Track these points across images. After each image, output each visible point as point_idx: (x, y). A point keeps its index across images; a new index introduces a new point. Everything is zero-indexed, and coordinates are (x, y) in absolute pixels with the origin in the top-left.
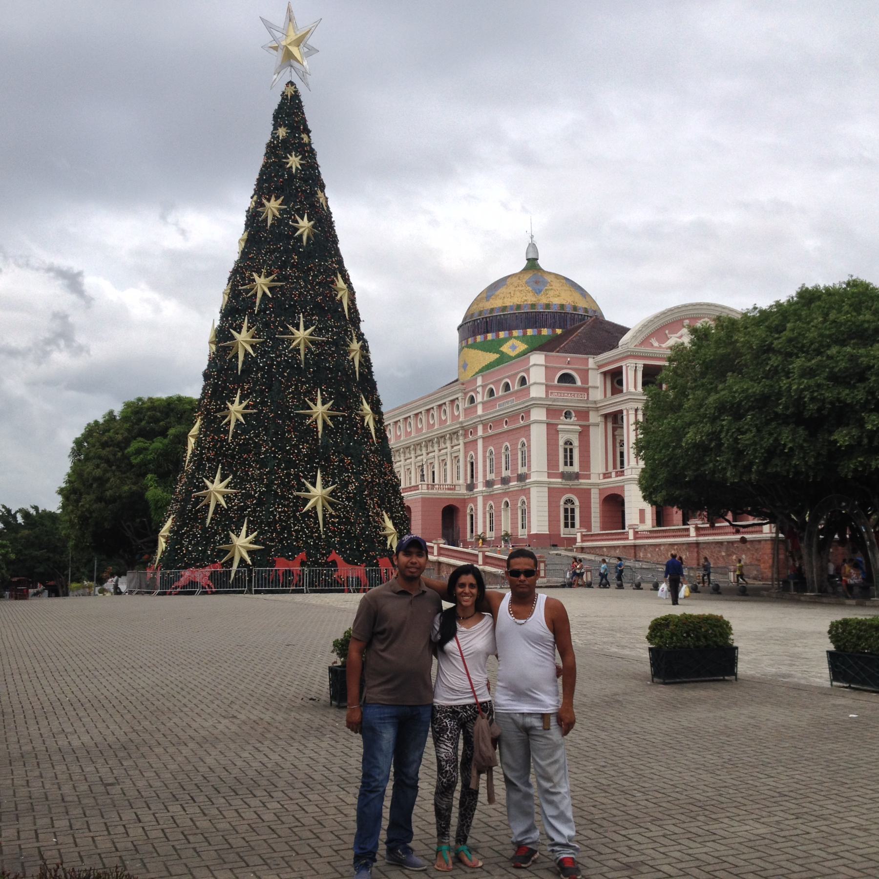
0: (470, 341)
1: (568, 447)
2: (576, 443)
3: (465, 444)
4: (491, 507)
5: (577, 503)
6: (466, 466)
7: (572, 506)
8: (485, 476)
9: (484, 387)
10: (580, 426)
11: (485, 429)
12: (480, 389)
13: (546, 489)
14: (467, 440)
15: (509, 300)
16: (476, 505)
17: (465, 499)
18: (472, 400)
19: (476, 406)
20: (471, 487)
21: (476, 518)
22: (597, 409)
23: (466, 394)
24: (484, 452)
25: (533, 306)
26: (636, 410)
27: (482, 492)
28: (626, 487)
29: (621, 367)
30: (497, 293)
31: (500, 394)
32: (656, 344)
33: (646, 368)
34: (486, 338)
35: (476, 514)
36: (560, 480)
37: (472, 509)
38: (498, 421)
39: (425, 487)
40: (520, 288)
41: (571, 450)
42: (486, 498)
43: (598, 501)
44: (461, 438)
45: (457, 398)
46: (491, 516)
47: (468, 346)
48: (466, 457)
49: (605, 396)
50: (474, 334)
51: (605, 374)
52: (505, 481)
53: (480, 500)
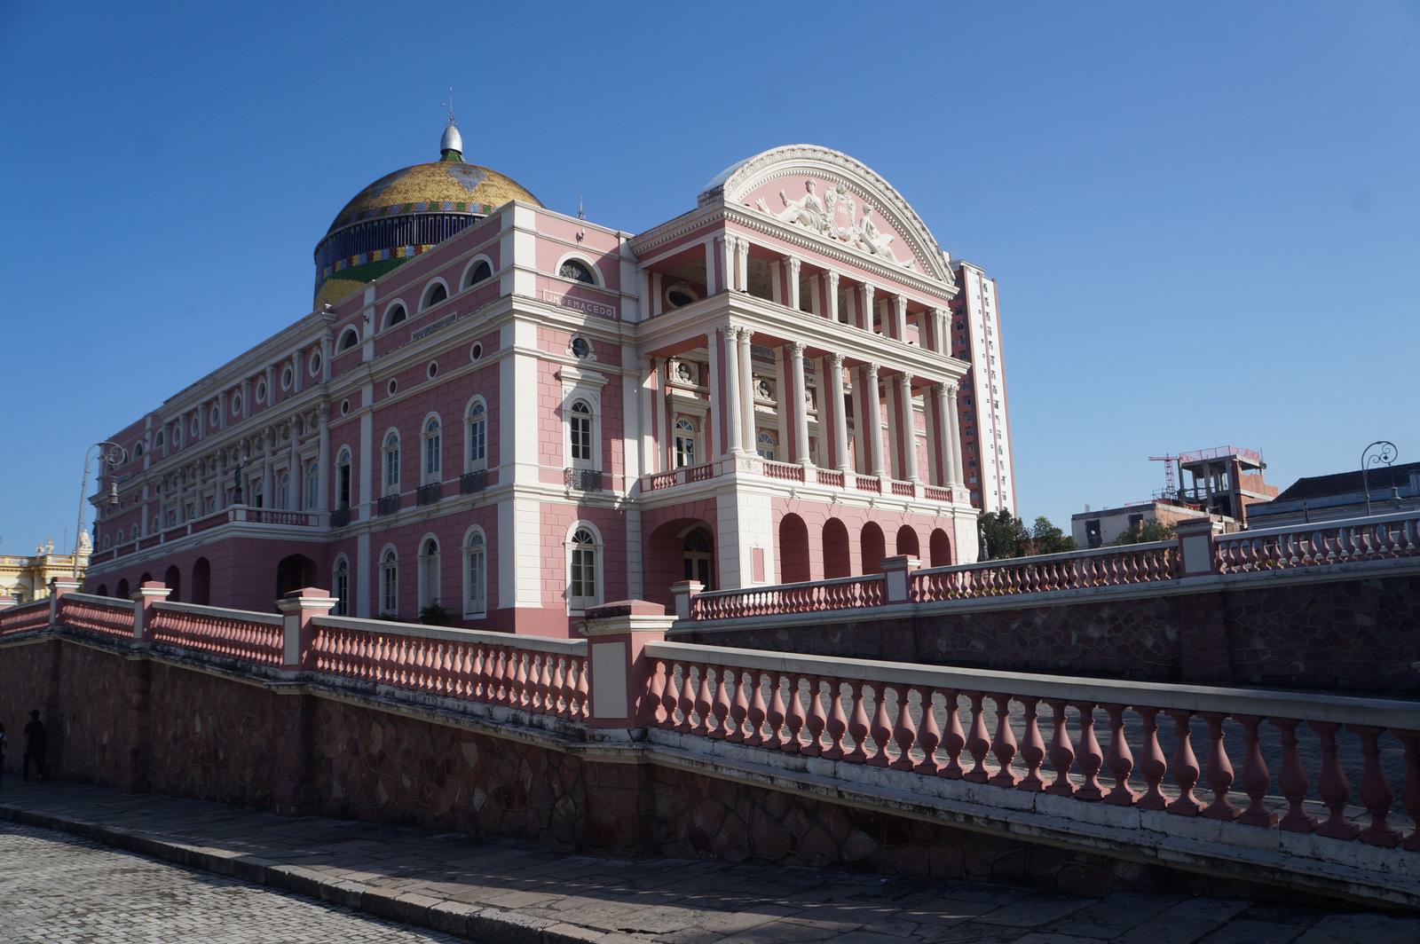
0: (340, 265)
1: (581, 416)
2: (596, 409)
3: (331, 431)
4: (391, 556)
5: (598, 539)
6: (331, 476)
7: (589, 548)
8: (376, 489)
9: (379, 309)
10: (604, 374)
11: (377, 395)
12: (370, 313)
13: (536, 506)
14: (335, 423)
15: (417, 194)
16: (354, 556)
17: (328, 544)
18: (351, 339)
19: (360, 351)
20: (342, 517)
21: (354, 582)
22: (638, 344)
23: (335, 332)
24: (376, 441)
25: (461, 205)
26: (740, 334)
27: (369, 524)
28: (721, 503)
29: (703, 246)
30: (393, 184)
31: (421, 310)
32: (767, 210)
34: (371, 257)
35: (354, 574)
36: (563, 488)
37: (343, 565)
38: (411, 375)
39: (242, 515)
40: (437, 178)
41: (586, 423)
42: (376, 541)
43: (638, 537)
44: (322, 419)
45: (318, 343)
46: (390, 574)
47: (335, 275)
48: (332, 457)
49: (652, 316)
50: (347, 254)
51: (651, 271)
52: (428, 495)
53: (364, 545)
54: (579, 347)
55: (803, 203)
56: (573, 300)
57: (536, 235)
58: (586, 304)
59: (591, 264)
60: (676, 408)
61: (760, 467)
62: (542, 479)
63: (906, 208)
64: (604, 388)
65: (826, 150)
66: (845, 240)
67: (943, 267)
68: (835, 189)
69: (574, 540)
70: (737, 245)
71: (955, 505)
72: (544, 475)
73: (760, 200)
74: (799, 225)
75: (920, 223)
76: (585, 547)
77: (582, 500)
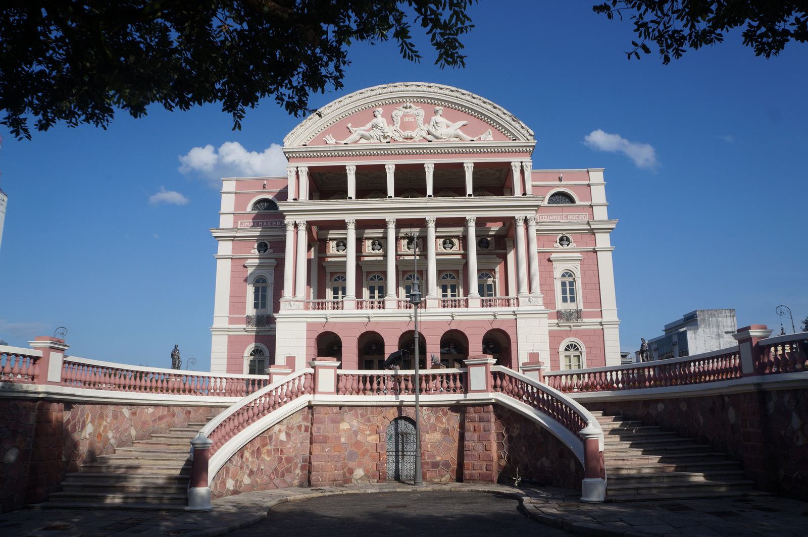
2: (270, 279)
7: (261, 358)
10: (276, 259)
26: (296, 226)
33: (309, 168)
36: (244, 326)
54: (262, 247)
55: (369, 125)
56: (258, 222)
57: (235, 193)
58: (267, 222)
59: (271, 198)
60: (329, 270)
61: (302, 305)
62: (230, 323)
63: (474, 98)
64: (276, 267)
65: (384, 86)
66: (411, 138)
67: (521, 130)
68: (401, 107)
69: (251, 354)
70: (297, 172)
71: (520, 308)
72: (232, 321)
73: (327, 137)
74: (363, 141)
75: (490, 104)
76: (258, 357)
77: (256, 332)
